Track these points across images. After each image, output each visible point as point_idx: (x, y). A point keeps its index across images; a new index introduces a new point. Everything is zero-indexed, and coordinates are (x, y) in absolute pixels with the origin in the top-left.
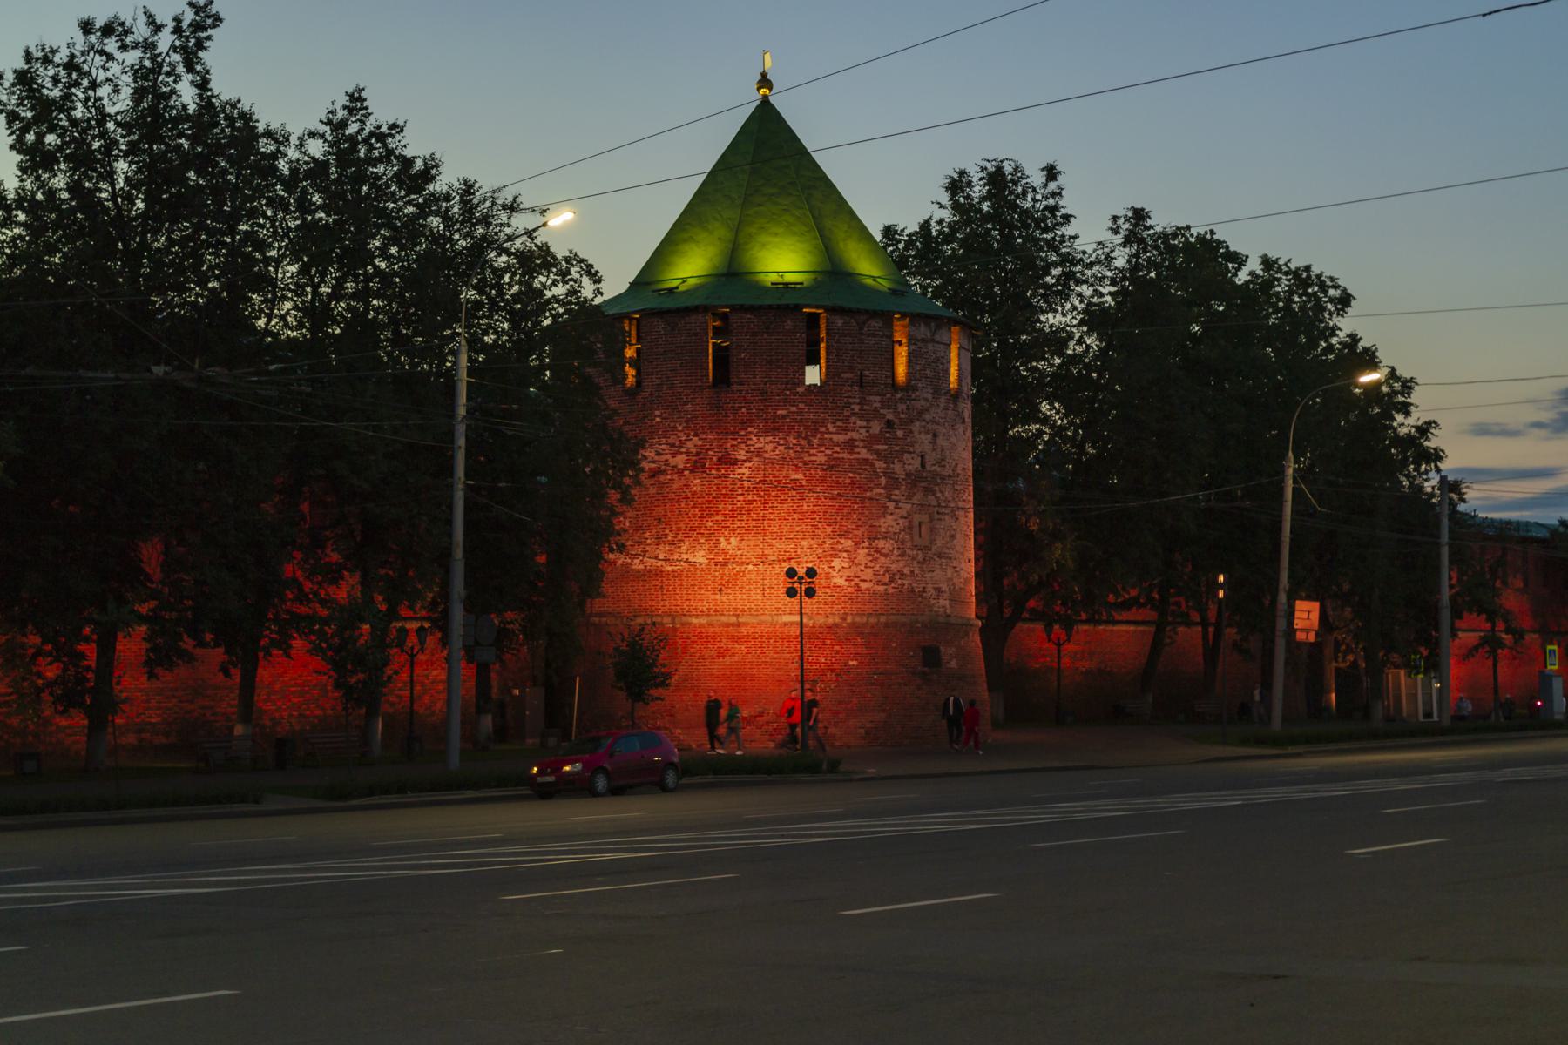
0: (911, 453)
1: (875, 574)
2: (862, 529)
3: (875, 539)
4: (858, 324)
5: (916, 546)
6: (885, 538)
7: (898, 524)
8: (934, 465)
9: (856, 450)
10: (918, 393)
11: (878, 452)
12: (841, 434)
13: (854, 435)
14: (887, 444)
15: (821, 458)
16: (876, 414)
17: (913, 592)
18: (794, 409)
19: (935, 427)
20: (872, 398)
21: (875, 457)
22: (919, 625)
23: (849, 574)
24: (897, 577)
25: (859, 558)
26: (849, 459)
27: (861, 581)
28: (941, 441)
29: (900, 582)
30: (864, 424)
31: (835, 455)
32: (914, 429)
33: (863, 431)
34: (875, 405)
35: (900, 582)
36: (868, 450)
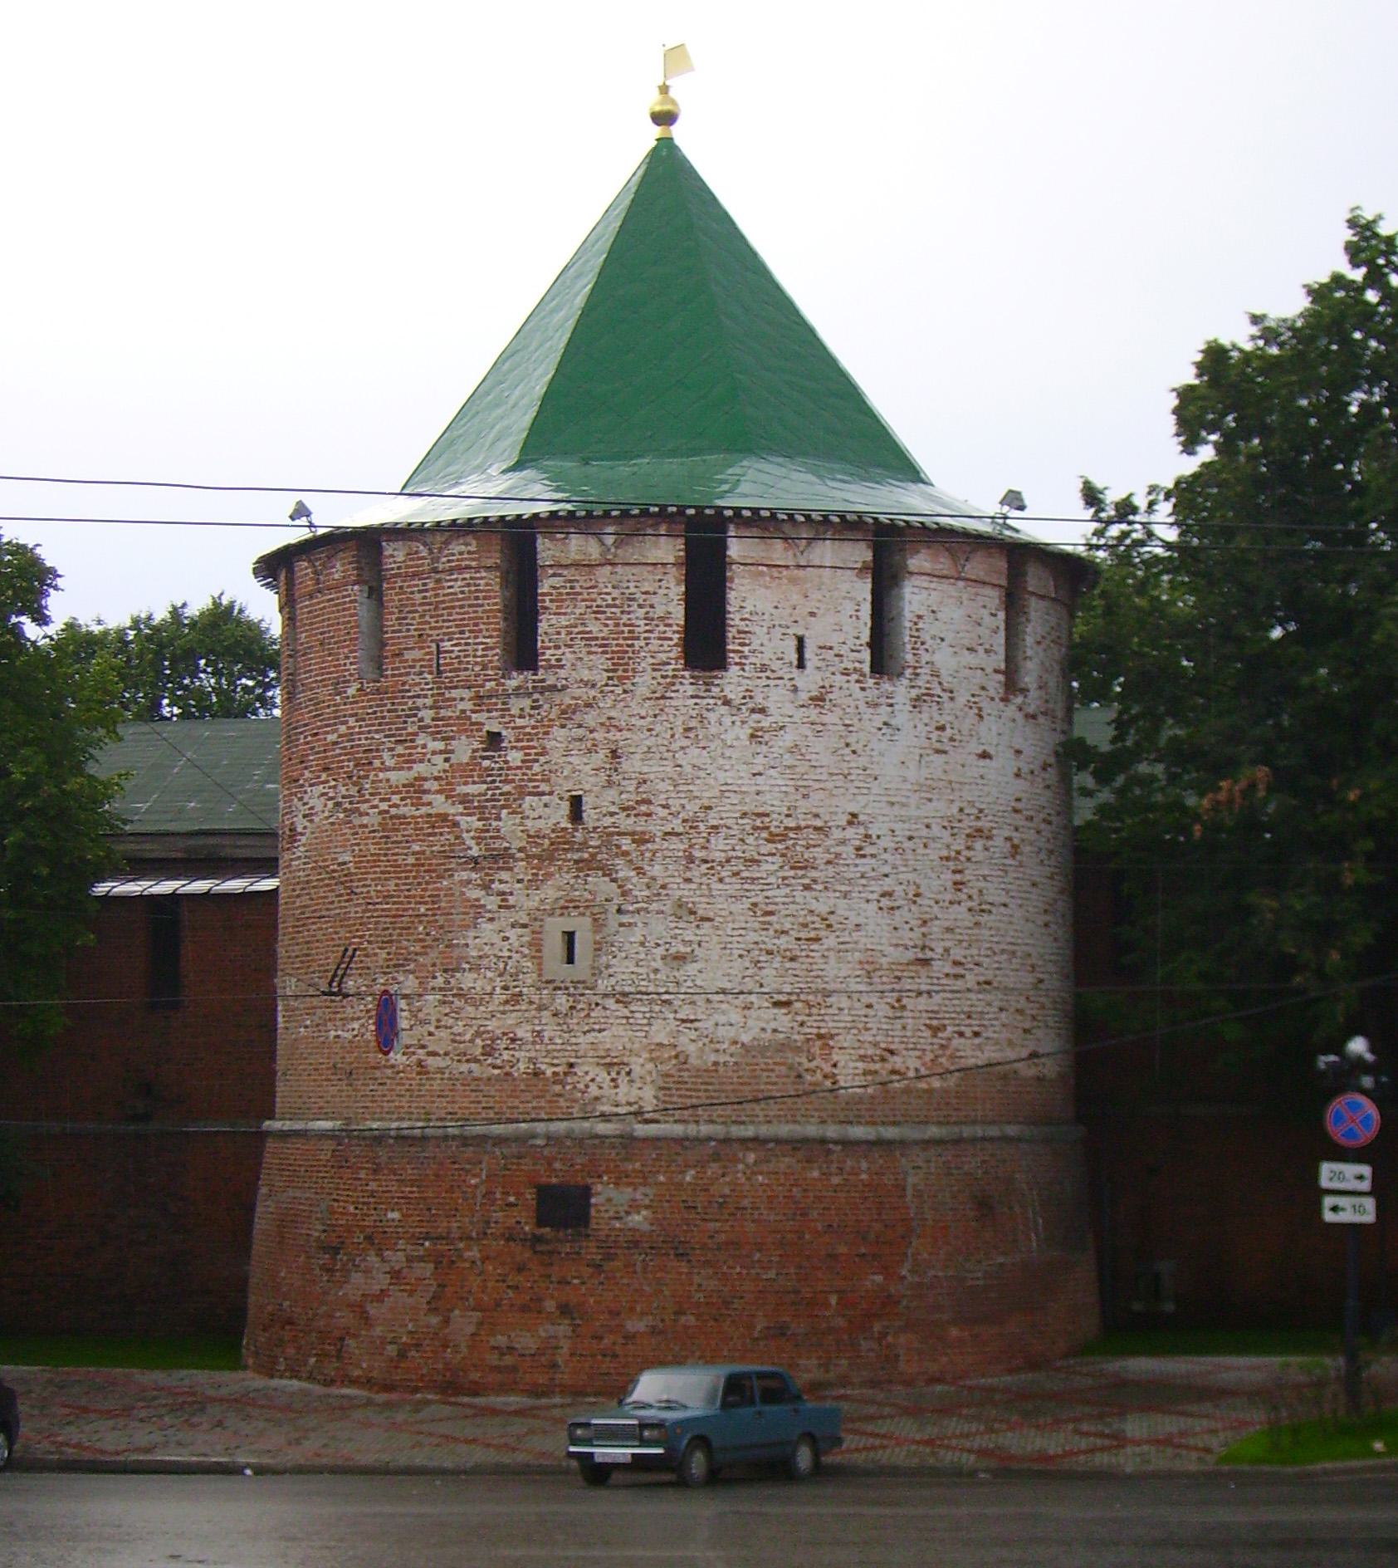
0: (543, 794)
1: (454, 1041)
2: (433, 954)
3: (453, 970)
4: (431, 551)
5: (548, 982)
6: (475, 968)
7: (506, 939)
8: (612, 814)
9: (426, 798)
10: (562, 673)
11: (465, 800)
12: (401, 769)
13: (420, 768)
14: (485, 782)
15: (373, 820)
16: (465, 724)
17: (537, 1074)
18: (343, 729)
19: (614, 735)
20: (455, 693)
21: (460, 808)
22: (540, 1142)
23: (409, 1042)
24: (502, 1044)
25: (425, 1011)
26: (413, 817)
27: (434, 1054)
28: (632, 765)
29: (506, 1055)
30: (440, 745)
31: (393, 811)
32: (549, 745)
33: (439, 759)
34: (462, 706)
35: (506, 1055)
36: (447, 797)
